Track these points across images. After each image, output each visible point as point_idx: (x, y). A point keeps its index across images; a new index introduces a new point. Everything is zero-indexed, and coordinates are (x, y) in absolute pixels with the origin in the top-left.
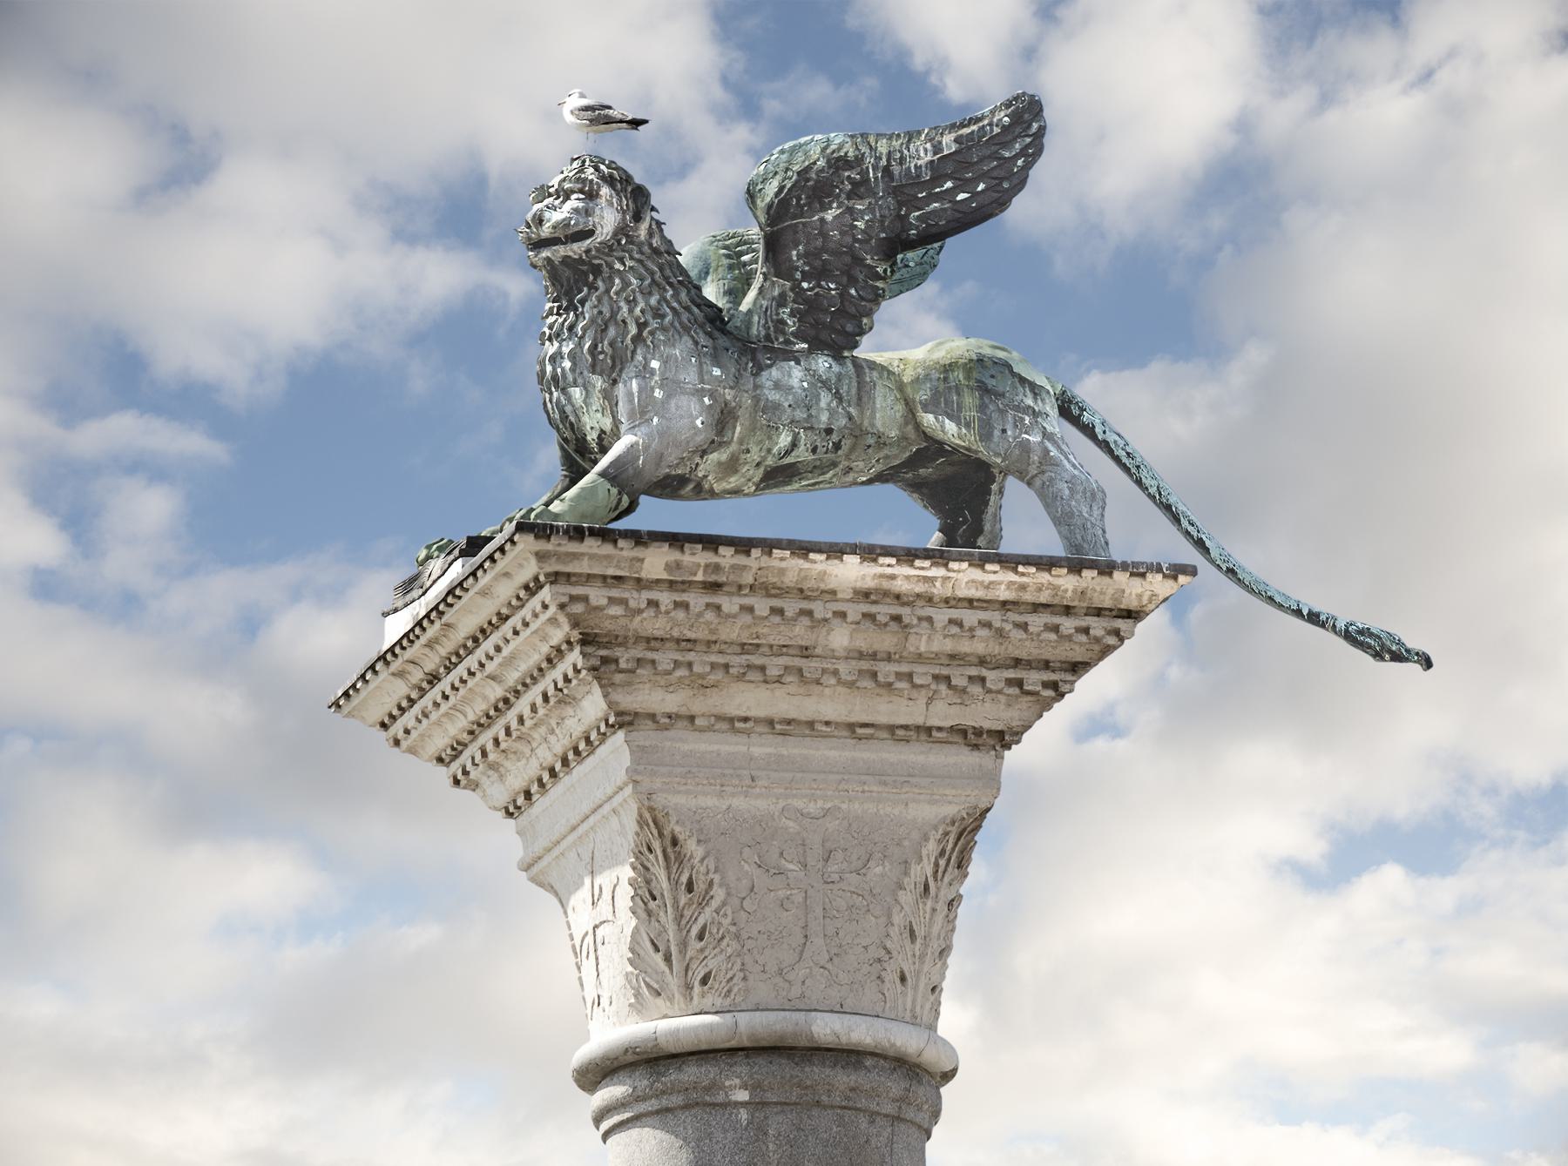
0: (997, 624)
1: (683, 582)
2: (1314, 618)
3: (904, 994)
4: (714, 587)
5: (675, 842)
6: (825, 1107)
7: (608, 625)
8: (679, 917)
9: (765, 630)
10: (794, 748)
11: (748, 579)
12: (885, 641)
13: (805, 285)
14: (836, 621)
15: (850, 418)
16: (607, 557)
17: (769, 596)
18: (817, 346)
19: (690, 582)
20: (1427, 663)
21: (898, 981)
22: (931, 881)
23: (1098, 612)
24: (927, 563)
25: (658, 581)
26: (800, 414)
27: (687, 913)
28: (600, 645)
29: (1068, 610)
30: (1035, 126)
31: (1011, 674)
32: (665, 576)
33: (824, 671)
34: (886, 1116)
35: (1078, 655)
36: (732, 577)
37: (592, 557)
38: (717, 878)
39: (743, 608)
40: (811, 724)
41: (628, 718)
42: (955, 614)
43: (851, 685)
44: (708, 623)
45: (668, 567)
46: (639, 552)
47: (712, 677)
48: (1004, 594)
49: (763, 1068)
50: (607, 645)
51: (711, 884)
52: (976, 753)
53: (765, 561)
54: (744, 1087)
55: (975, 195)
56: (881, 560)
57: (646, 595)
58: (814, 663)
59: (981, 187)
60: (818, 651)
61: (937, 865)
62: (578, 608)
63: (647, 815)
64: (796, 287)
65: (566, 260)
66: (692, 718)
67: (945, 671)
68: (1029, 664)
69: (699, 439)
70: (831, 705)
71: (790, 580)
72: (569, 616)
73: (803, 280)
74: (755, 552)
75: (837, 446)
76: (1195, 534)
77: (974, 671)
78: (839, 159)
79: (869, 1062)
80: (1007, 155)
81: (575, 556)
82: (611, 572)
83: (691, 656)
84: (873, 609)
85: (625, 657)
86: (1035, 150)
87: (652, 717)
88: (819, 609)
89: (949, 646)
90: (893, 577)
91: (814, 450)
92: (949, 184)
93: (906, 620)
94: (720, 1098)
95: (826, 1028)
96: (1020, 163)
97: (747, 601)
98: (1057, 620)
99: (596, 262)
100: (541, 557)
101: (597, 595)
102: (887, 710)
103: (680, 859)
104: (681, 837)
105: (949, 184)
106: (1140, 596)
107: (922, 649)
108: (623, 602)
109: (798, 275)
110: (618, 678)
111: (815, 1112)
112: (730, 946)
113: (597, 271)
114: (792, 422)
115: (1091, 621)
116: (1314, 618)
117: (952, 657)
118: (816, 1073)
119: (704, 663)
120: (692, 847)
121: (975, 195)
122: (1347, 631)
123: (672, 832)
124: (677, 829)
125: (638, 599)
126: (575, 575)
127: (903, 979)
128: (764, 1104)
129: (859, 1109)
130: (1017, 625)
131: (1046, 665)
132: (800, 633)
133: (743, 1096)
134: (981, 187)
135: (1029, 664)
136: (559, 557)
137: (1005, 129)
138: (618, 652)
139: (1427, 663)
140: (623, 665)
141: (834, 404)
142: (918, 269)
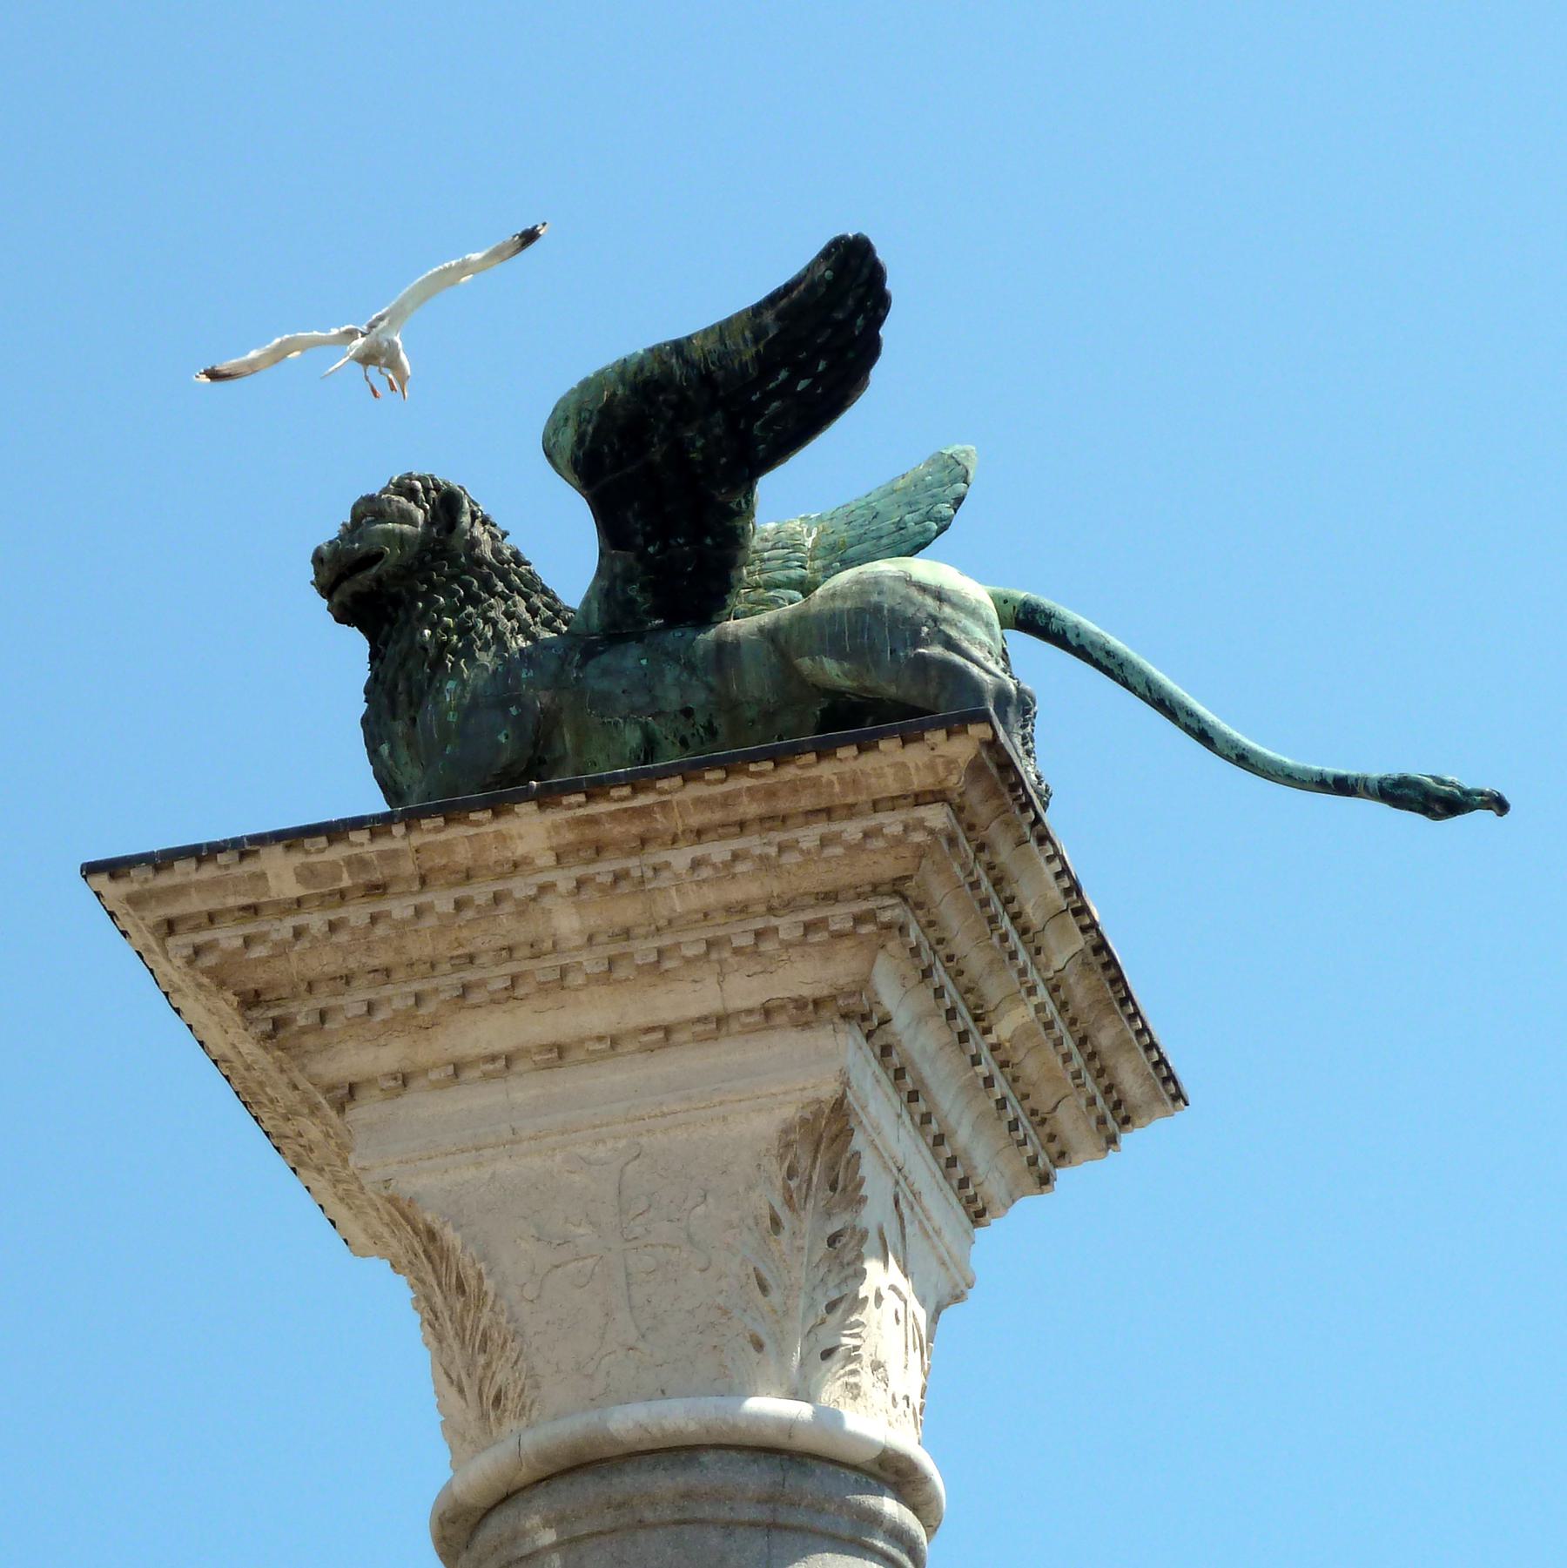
0: (758, 852)
2: (1342, 786)
4: (377, 889)
5: (432, 1235)
6: (653, 1526)
7: (258, 978)
8: (460, 1334)
9: (465, 933)
10: (568, 1081)
11: (408, 867)
12: (627, 911)
13: (651, 549)
15: (711, 689)
16: (216, 883)
17: (452, 885)
19: (342, 894)
20: (1499, 805)
22: (784, 1214)
23: (894, 802)
24: (626, 791)
25: (299, 902)
26: (641, 699)
27: (468, 1324)
28: (269, 1004)
29: (851, 811)
30: (866, 271)
31: (809, 916)
32: (298, 891)
34: (753, 1524)
35: (888, 868)
36: (387, 871)
37: (200, 886)
38: (482, 1266)
39: (419, 912)
42: (699, 851)
44: (385, 940)
45: (306, 874)
46: (249, 866)
47: (422, 1011)
48: (750, 809)
49: (570, 1495)
51: (480, 1277)
52: (808, 1034)
53: (416, 839)
54: (547, 1524)
55: (818, 379)
56: (566, 800)
57: (290, 922)
58: (549, 962)
59: (822, 366)
61: (787, 1189)
62: (209, 960)
63: (393, 1210)
64: (642, 556)
65: (357, 598)
67: (720, 932)
68: (830, 897)
69: (505, 758)
70: (593, 1014)
71: (463, 856)
72: (207, 972)
73: (648, 543)
74: (398, 830)
75: (711, 730)
76: (1195, 725)
77: (759, 924)
78: (646, 383)
79: (707, 1458)
80: (840, 316)
81: (179, 891)
82: (232, 901)
83: (388, 990)
84: (591, 870)
85: (303, 1015)
87: (371, 1081)
88: (521, 887)
89: (710, 896)
90: (592, 820)
91: (684, 743)
92: (783, 374)
93: (636, 873)
94: (526, 1549)
95: (628, 1420)
96: (860, 321)
98: (835, 827)
99: (394, 590)
100: (134, 901)
101: (228, 937)
103: (445, 1254)
104: (437, 1226)
105: (783, 374)
106: (931, 767)
108: (262, 938)
109: (640, 540)
110: (310, 1041)
111: (641, 1536)
112: (512, 1350)
113: (396, 601)
114: (633, 710)
115: (882, 818)
116: (1342, 786)
117: (729, 909)
118: (626, 1483)
119: (405, 996)
120: (451, 1237)
122: (1381, 789)
123: (425, 1224)
124: (429, 1217)
126: (190, 917)
128: (575, 1540)
129: (702, 1522)
132: (507, 926)
133: (548, 1537)
134: (822, 366)
135: (830, 897)
136: (160, 896)
137: (830, 285)
138: (293, 1007)
139: (1499, 805)
140: (301, 1021)
141: (685, 677)
142: (917, 528)
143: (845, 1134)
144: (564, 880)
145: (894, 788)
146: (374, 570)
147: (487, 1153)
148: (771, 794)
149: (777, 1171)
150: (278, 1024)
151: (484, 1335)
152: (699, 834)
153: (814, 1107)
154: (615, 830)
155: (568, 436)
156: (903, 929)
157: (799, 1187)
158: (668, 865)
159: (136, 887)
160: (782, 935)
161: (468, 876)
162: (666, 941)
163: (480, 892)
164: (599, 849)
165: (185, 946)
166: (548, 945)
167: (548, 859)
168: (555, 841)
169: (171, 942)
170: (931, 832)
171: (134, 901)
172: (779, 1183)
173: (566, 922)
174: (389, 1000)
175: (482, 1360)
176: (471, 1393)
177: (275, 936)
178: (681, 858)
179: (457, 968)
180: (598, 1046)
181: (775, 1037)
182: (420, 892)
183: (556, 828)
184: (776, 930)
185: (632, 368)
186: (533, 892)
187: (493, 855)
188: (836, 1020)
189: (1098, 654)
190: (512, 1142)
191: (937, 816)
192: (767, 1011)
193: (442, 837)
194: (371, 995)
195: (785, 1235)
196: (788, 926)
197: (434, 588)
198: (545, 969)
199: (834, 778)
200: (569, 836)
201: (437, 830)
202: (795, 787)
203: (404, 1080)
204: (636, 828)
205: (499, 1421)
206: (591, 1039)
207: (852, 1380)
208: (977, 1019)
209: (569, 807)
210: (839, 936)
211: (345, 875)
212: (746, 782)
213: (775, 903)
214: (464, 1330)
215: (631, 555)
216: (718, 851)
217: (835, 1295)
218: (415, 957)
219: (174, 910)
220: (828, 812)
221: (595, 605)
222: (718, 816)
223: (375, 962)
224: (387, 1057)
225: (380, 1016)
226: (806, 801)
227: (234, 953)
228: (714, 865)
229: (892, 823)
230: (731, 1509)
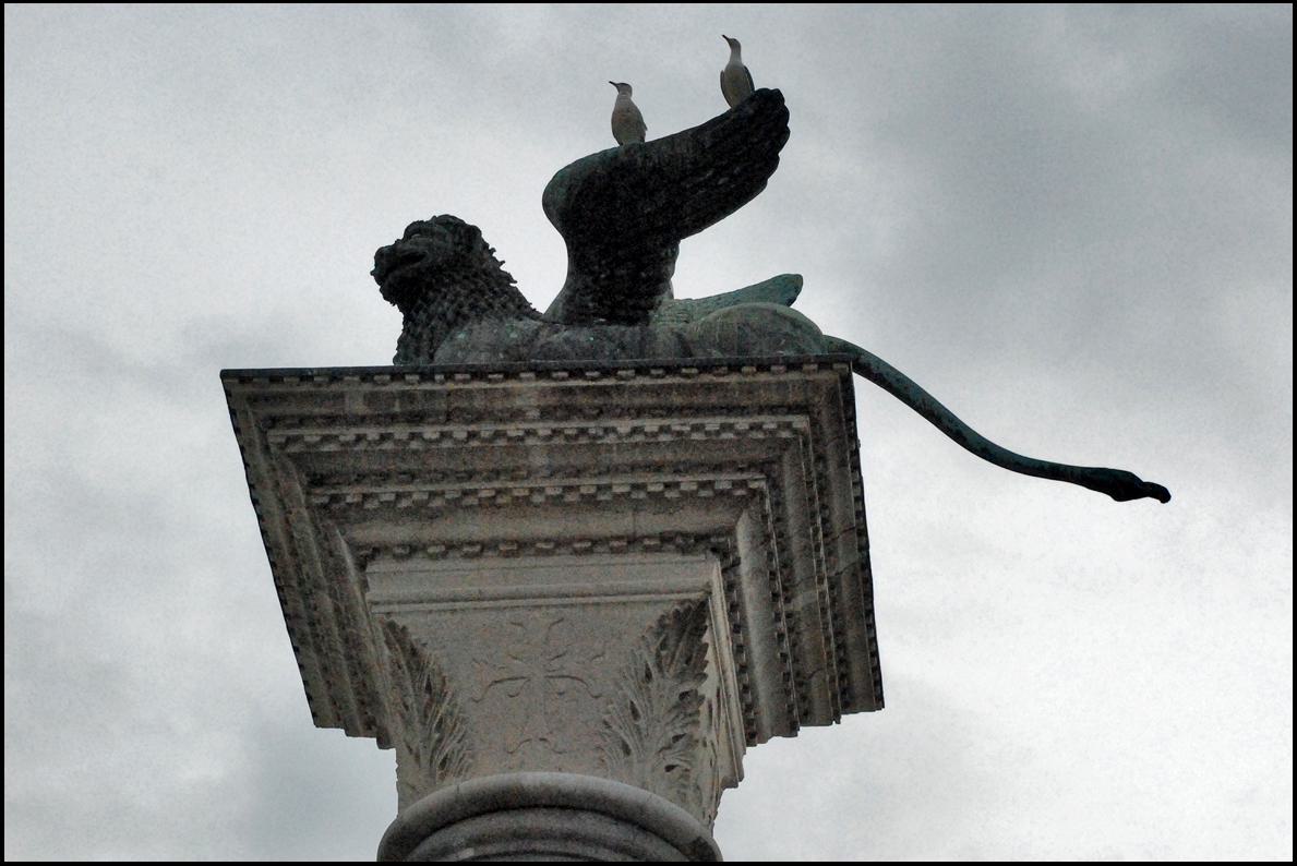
0: (678, 428)
1: (386, 416)
3: (629, 764)
4: (417, 418)
5: (414, 652)
11: (442, 405)
14: (530, 442)
18: (612, 319)
20: (1162, 494)
21: (622, 754)
22: (654, 671)
23: (772, 409)
24: (596, 374)
29: (742, 411)
33: (532, 490)
35: (760, 454)
39: (443, 435)
40: (533, 544)
41: (369, 552)
42: (637, 423)
43: (556, 501)
44: (415, 452)
45: (370, 399)
48: (677, 400)
50: (334, 486)
52: (689, 558)
53: (450, 386)
55: (733, 177)
60: (524, 473)
61: (658, 655)
62: (294, 449)
66: (424, 548)
67: (641, 481)
68: (718, 468)
71: (479, 403)
76: (954, 429)
77: (669, 479)
81: (283, 398)
84: (562, 425)
86: (781, 134)
88: (513, 429)
90: (570, 391)
95: (535, 777)
97: (446, 429)
101: (312, 435)
102: (597, 525)
104: (418, 647)
107: (617, 458)
115: (761, 419)
121: (733, 177)
123: (412, 645)
125: (349, 434)
126: (284, 417)
127: (627, 751)
130: (696, 428)
131: (734, 466)
134: (737, 170)
137: (751, 119)
138: (345, 490)
139: (1162, 494)
143: (699, 630)
144: (543, 429)
145: (775, 399)
146: (416, 265)
147: (458, 605)
148: (692, 390)
149: (655, 645)
150: (334, 499)
151: (441, 722)
152: (640, 412)
153: (686, 605)
154: (582, 400)
155: (561, 196)
156: (763, 497)
157: (666, 657)
158: (614, 430)
159: (255, 390)
160: (683, 487)
161: (479, 417)
162: (604, 481)
163: (486, 429)
164: (571, 411)
165: (282, 436)
166: (524, 473)
167: (535, 413)
168: (543, 403)
169: (271, 432)
170: (795, 431)
171: (253, 400)
172: (653, 650)
173: (539, 460)
174: (410, 494)
175: (437, 736)
176: (424, 760)
177: (342, 438)
178: (624, 426)
179: (460, 480)
180: (544, 546)
181: (666, 557)
182: (445, 424)
183: (543, 393)
184: (677, 484)
185: (609, 155)
186: (521, 433)
187: (498, 405)
188: (708, 551)
189: (891, 379)
190: (479, 599)
191: (800, 422)
192: (666, 539)
193: (467, 386)
194: (400, 489)
195: (653, 686)
196: (688, 483)
197: (454, 281)
198: (520, 489)
199: (737, 387)
200: (552, 400)
201: (465, 381)
202: (709, 389)
203: (413, 549)
204: (599, 401)
205: (443, 777)
206: (539, 540)
207: (683, 790)
208: (785, 589)
209: (555, 380)
210: (722, 493)
211: (397, 403)
212: (677, 380)
213: (681, 467)
214: (426, 716)
215: (589, 279)
216: (651, 425)
217: (679, 732)
218: (433, 467)
219: (277, 411)
220: (730, 410)
221: (561, 305)
222: (650, 400)
223: (404, 467)
224: (403, 532)
225: (404, 503)
226: (714, 399)
227: (315, 445)
228: (646, 434)
229: (770, 423)
230: (596, 852)
